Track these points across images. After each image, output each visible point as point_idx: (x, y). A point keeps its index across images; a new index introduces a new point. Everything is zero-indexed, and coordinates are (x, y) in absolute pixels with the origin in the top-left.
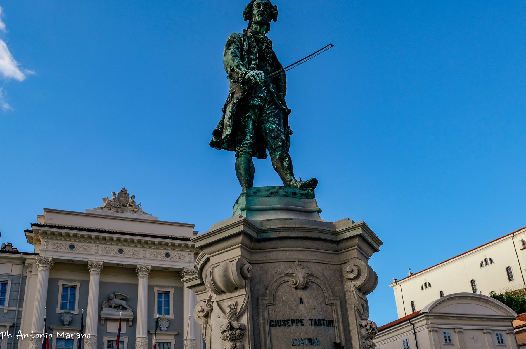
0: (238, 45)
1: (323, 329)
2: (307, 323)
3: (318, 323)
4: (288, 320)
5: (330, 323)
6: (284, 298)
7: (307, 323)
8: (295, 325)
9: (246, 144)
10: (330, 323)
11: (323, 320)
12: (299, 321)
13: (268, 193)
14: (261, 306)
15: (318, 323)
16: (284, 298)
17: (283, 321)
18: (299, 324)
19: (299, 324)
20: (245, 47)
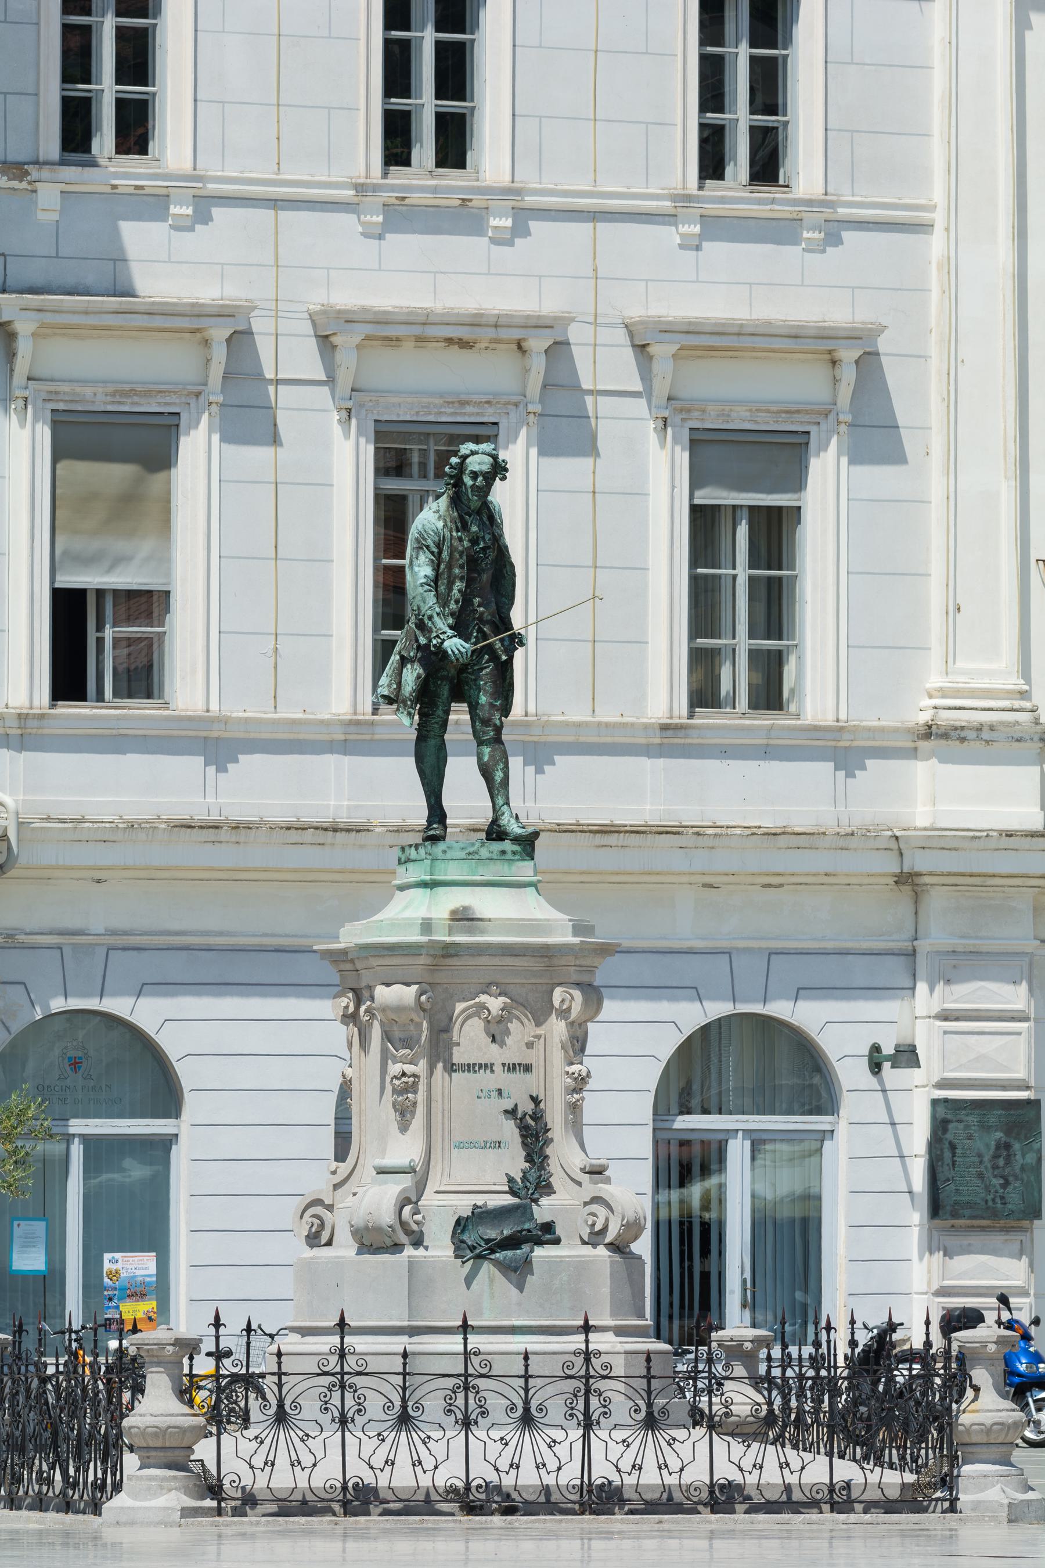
0: (432, 553)
1: (519, 1076)
2: (498, 1068)
3: (512, 1068)
4: (474, 1065)
5: (528, 1068)
6: (472, 1034)
7: (498, 1068)
8: (482, 1071)
9: (436, 723)
10: (528, 1068)
11: (519, 1065)
12: (489, 1067)
13: (463, 855)
14: (441, 1044)
15: (512, 1068)
16: (472, 1034)
17: (469, 1065)
18: (488, 1071)
19: (488, 1071)
20: (445, 555)
